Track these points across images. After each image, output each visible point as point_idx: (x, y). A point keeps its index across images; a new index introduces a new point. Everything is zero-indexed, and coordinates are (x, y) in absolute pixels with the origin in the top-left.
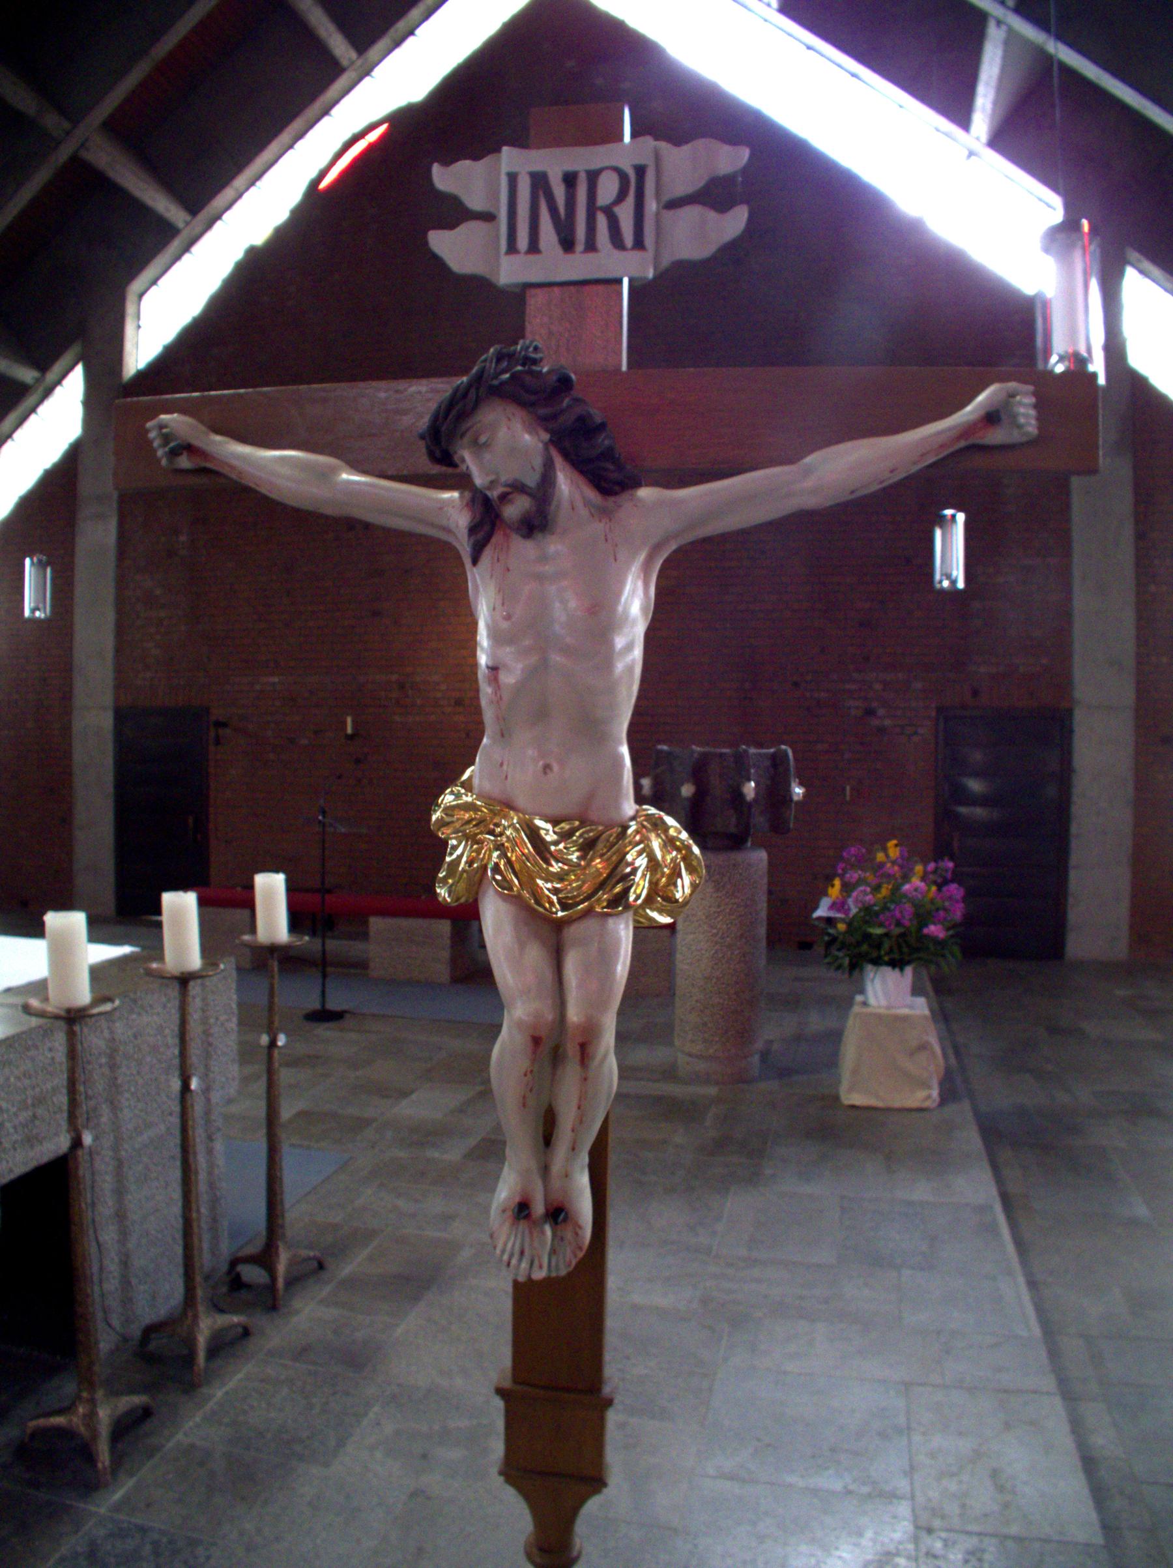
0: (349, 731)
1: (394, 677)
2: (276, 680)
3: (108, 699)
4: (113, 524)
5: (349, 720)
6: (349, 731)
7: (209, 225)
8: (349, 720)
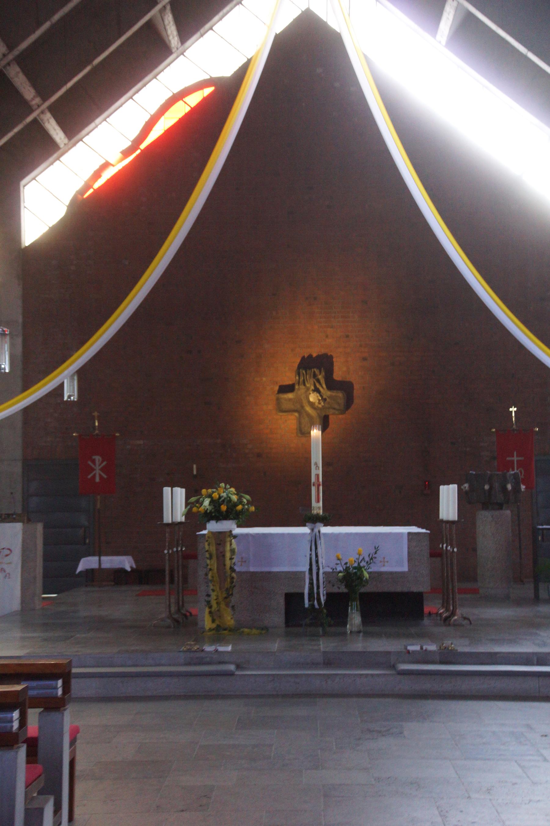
0: (195, 473)
1: (219, 441)
2: (141, 442)
3: (18, 453)
5: (195, 466)
6: (195, 473)
7: (75, 145)
8: (195, 466)
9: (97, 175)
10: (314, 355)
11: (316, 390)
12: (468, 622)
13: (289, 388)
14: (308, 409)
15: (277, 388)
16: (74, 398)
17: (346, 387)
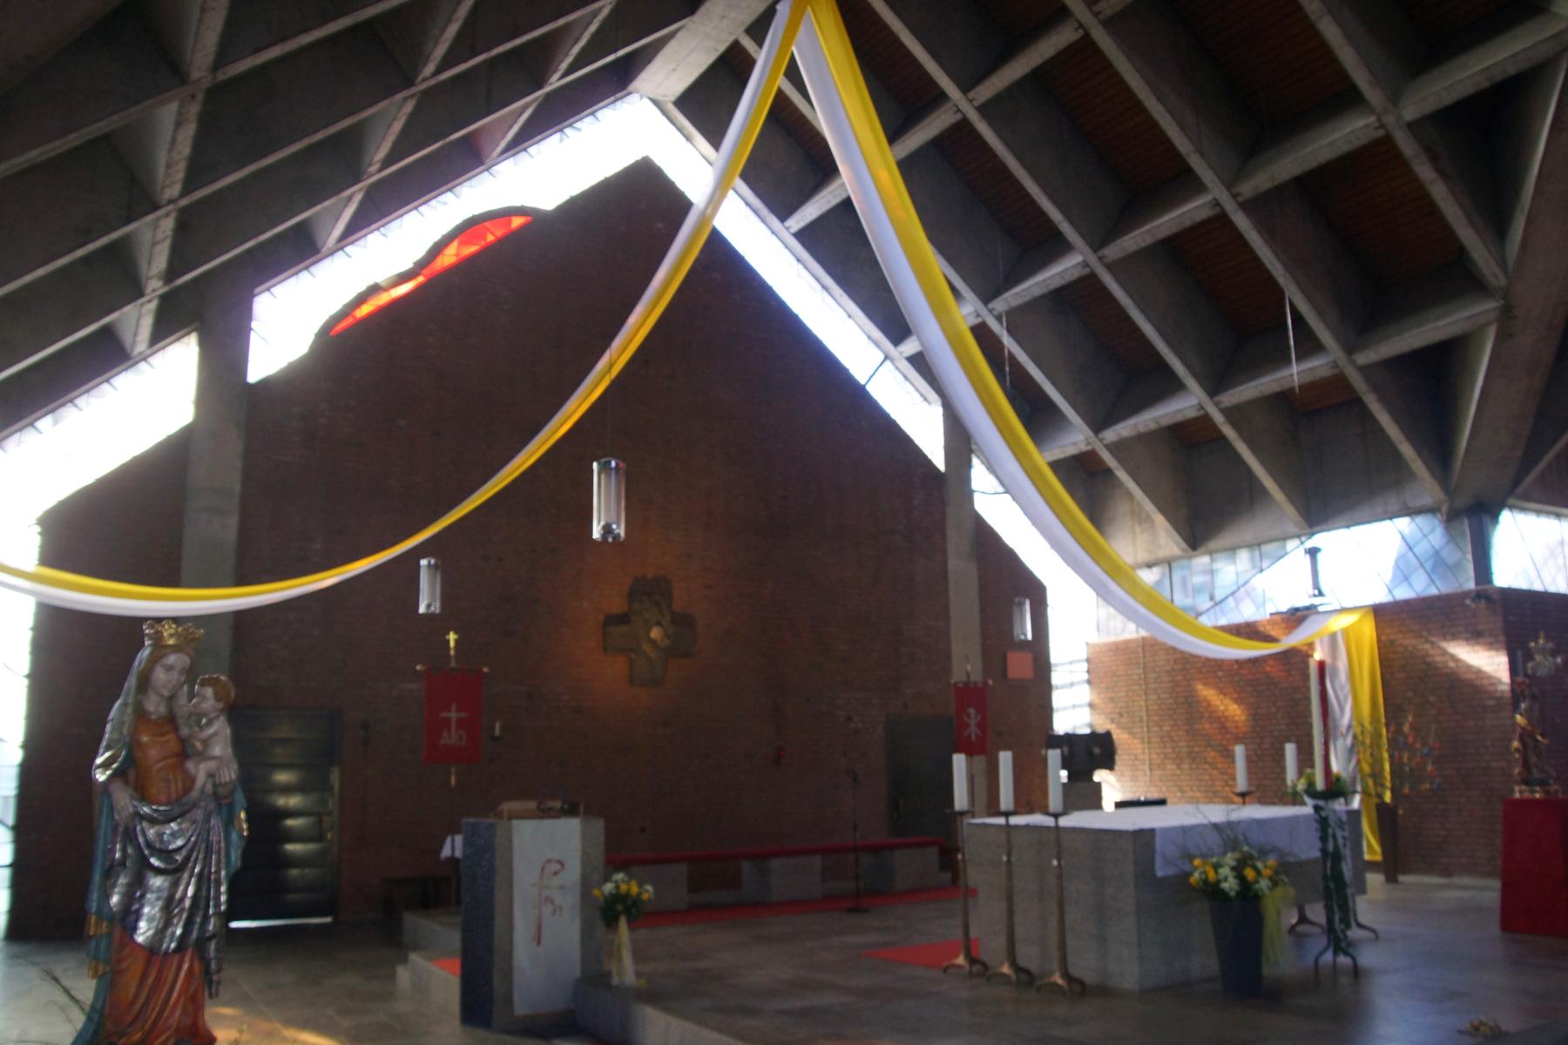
0: (497, 732)
4: (233, 521)
6: (497, 732)
9: (361, 299)
10: (650, 576)
11: (658, 624)
12: (1371, 935)
13: (624, 619)
14: (646, 647)
15: (601, 618)
16: (436, 608)
17: (682, 622)
